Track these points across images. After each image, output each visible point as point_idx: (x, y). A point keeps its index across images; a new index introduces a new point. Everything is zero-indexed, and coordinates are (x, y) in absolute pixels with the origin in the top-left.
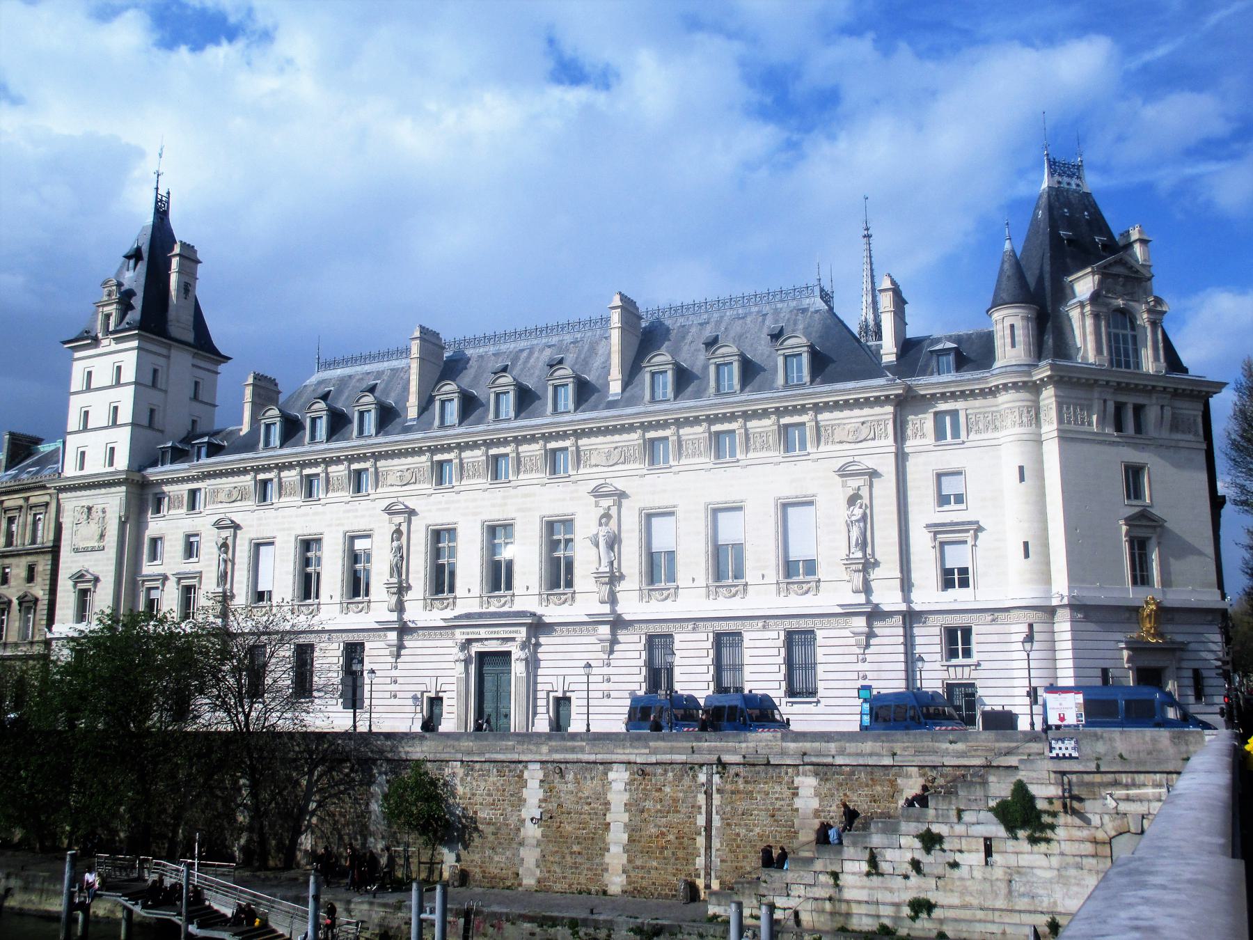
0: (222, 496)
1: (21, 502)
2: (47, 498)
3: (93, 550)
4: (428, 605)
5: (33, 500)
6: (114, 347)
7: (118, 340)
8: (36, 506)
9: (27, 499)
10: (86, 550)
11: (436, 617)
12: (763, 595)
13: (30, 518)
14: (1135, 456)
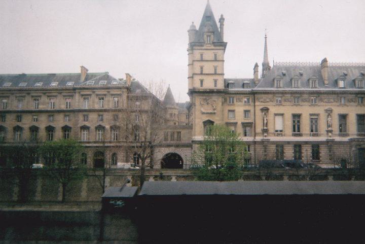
2: (121, 92)
3: (211, 113)
6: (213, 47)
7: (215, 46)
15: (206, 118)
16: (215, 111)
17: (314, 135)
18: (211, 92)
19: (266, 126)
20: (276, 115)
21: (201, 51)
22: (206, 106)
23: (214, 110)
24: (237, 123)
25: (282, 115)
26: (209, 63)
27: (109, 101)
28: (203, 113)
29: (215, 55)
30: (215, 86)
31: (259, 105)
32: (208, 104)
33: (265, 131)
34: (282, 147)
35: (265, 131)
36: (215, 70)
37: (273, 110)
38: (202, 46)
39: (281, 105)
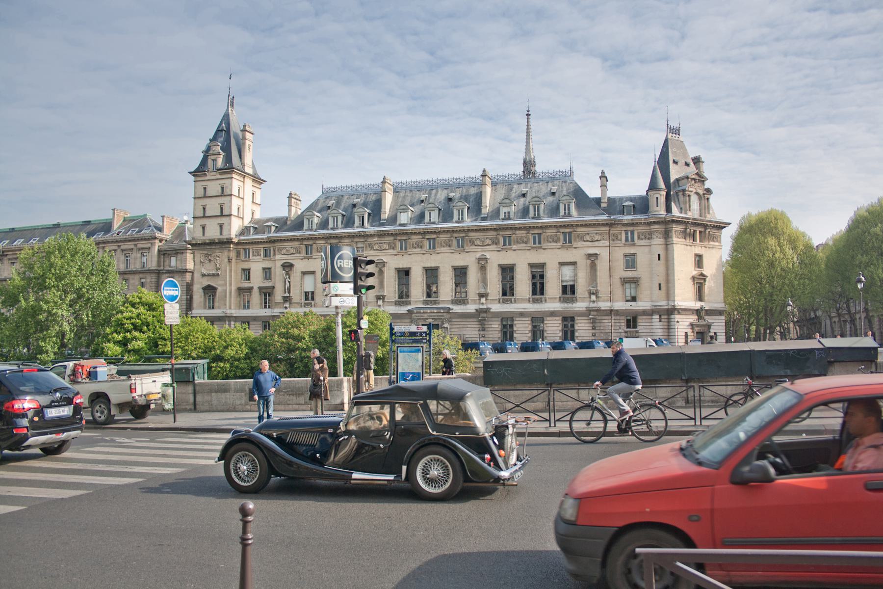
0: (284, 251)
1: (132, 246)
2: (149, 245)
3: (214, 275)
4: (397, 303)
5: (140, 246)
6: (219, 177)
7: (221, 174)
8: (142, 249)
9: (136, 245)
10: (209, 275)
11: (403, 310)
12: (552, 303)
13: (139, 255)
14: (698, 250)
15: (206, 282)
16: (219, 272)
17: (535, 301)
18: (212, 243)
19: (289, 292)
20: (304, 273)
21: (204, 183)
22: (207, 265)
23: (217, 269)
24: (252, 288)
25: (313, 273)
26: (214, 199)
27: (136, 258)
28: (203, 275)
29: (222, 188)
30: (221, 234)
31: (280, 259)
32: (210, 260)
33: (287, 299)
34: (572, 319)
35: (287, 299)
36: (222, 209)
37: (300, 265)
38: (205, 175)
39: (311, 258)
